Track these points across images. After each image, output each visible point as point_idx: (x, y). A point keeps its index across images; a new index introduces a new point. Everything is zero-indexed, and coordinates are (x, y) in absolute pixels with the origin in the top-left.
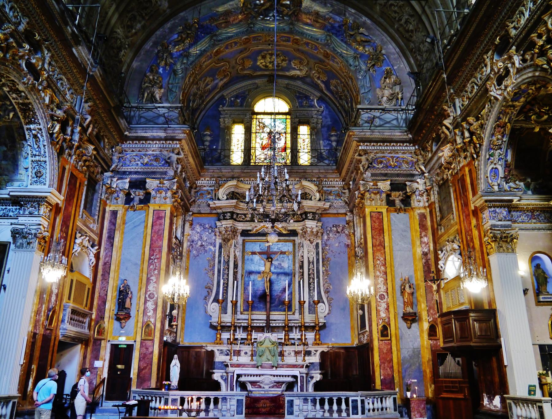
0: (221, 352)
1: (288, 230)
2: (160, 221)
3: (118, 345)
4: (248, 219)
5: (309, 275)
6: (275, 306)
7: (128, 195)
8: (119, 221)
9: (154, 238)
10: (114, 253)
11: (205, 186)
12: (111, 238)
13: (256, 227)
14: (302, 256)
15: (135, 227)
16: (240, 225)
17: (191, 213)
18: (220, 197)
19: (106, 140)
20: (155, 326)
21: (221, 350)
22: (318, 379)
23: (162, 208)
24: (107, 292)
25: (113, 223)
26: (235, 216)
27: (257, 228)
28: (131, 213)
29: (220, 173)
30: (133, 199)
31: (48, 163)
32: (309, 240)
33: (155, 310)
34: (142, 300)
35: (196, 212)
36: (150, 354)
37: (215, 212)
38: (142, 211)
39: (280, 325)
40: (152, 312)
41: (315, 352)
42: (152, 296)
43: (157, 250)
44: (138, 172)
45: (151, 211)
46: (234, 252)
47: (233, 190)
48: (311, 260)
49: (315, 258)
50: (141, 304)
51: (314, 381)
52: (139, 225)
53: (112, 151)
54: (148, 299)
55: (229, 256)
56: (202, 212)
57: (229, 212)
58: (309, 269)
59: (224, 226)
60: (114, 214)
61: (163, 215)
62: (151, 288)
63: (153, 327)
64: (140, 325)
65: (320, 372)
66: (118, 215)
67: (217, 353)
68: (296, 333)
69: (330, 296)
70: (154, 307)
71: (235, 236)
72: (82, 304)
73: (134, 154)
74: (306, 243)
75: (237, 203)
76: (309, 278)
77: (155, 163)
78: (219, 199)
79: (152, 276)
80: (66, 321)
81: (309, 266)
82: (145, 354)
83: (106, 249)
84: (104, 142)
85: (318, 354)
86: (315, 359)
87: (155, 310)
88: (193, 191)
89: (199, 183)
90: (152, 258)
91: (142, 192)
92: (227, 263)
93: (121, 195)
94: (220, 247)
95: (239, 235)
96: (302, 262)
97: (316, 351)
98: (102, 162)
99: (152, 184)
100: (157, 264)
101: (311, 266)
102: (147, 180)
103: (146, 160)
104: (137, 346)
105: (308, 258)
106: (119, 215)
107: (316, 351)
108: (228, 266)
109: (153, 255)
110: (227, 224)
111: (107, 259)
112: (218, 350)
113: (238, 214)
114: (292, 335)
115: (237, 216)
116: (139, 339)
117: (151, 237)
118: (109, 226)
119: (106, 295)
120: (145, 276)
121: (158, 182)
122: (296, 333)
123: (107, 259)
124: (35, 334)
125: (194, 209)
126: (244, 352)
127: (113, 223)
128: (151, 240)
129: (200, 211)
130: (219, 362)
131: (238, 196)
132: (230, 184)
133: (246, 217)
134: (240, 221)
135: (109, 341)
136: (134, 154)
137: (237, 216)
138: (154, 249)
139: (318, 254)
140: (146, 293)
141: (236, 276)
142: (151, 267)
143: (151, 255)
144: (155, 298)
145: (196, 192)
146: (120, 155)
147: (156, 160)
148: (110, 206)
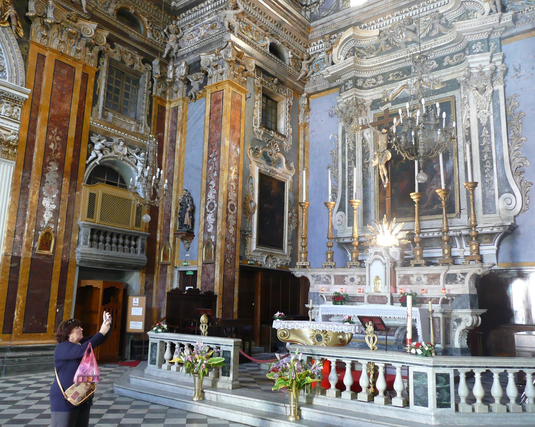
0: (318, 279)
1: (443, 83)
2: (218, 106)
3: (185, 272)
4: (381, 82)
5: (481, 148)
6: (427, 208)
7: (188, 83)
8: (179, 118)
9: (212, 130)
10: (176, 159)
11: (320, 53)
12: (173, 141)
13: (392, 90)
14: (469, 119)
15: (196, 121)
16: (369, 94)
17: (304, 95)
18: (335, 60)
19: (146, 20)
20: (215, 246)
21: (317, 276)
22: (469, 324)
23: (220, 88)
24: (171, 208)
25: (174, 123)
26: (360, 83)
27: (394, 92)
28: (193, 105)
29: (333, 27)
30: (192, 87)
31: (3, 51)
32: (477, 89)
33: (215, 224)
34: (203, 214)
35: (312, 91)
36: (211, 282)
37: (334, 84)
38: (203, 99)
39: (436, 234)
40: (212, 226)
41: (462, 276)
42: (211, 206)
43: (216, 146)
44: (195, 50)
45: (209, 96)
46: (362, 135)
47: (352, 44)
48: (484, 122)
49: (492, 117)
50: (201, 218)
51: (462, 326)
52: (200, 118)
53: (165, 33)
54: (208, 211)
55: (354, 143)
56: (319, 89)
57: (350, 79)
58: (481, 139)
59: (345, 101)
60: (176, 109)
61: (221, 96)
62: (211, 196)
63: (213, 247)
64: (201, 244)
65: (469, 311)
66: (179, 112)
67: (312, 281)
68: (461, 247)
69: (527, 179)
70: (214, 220)
71: (361, 111)
72: (127, 223)
73: (192, 29)
74: (472, 95)
75: (355, 61)
76: (481, 154)
77: (212, 33)
78: (333, 64)
79: (211, 180)
80: (81, 243)
81: (480, 133)
82: (206, 281)
83: (168, 156)
84: (143, 22)
85: (467, 278)
86: (464, 288)
87: (215, 224)
88: (304, 63)
89: (311, 50)
90: (211, 156)
91: (200, 75)
92: (353, 153)
93: (181, 85)
94: (344, 133)
95: (369, 109)
96: (469, 129)
97: (464, 274)
98: (139, 47)
99: (206, 58)
100: (216, 165)
101: (485, 131)
102: (202, 57)
103: (203, 32)
104: (199, 274)
105: (479, 120)
106: (180, 112)
107: (464, 274)
108: (355, 156)
109: (212, 152)
110: (348, 96)
111: (170, 168)
112: (313, 276)
113: (365, 79)
114: (456, 252)
115: (364, 82)
116: (200, 264)
117: (210, 130)
118: (171, 128)
119: (170, 212)
120: (204, 181)
121: (214, 55)
122: (461, 247)
123: (170, 168)
124: (16, 259)
125: (309, 88)
126: (350, 277)
127: (174, 123)
128: (210, 133)
129: (316, 88)
130: (314, 293)
131: (362, 51)
132: (345, 38)
133: (377, 80)
134: (369, 88)
135: (176, 267)
136: (192, 29)
137: (364, 82)
138: (213, 144)
139: (496, 109)
140: (206, 204)
141: (367, 169)
142: (210, 169)
143: (210, 153)
144: (215, 209)
145: (310, 64)
146: (178, 36)
147: (212, 28)
148: (170, 102)
